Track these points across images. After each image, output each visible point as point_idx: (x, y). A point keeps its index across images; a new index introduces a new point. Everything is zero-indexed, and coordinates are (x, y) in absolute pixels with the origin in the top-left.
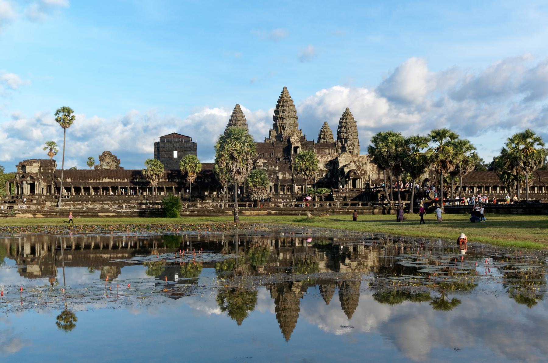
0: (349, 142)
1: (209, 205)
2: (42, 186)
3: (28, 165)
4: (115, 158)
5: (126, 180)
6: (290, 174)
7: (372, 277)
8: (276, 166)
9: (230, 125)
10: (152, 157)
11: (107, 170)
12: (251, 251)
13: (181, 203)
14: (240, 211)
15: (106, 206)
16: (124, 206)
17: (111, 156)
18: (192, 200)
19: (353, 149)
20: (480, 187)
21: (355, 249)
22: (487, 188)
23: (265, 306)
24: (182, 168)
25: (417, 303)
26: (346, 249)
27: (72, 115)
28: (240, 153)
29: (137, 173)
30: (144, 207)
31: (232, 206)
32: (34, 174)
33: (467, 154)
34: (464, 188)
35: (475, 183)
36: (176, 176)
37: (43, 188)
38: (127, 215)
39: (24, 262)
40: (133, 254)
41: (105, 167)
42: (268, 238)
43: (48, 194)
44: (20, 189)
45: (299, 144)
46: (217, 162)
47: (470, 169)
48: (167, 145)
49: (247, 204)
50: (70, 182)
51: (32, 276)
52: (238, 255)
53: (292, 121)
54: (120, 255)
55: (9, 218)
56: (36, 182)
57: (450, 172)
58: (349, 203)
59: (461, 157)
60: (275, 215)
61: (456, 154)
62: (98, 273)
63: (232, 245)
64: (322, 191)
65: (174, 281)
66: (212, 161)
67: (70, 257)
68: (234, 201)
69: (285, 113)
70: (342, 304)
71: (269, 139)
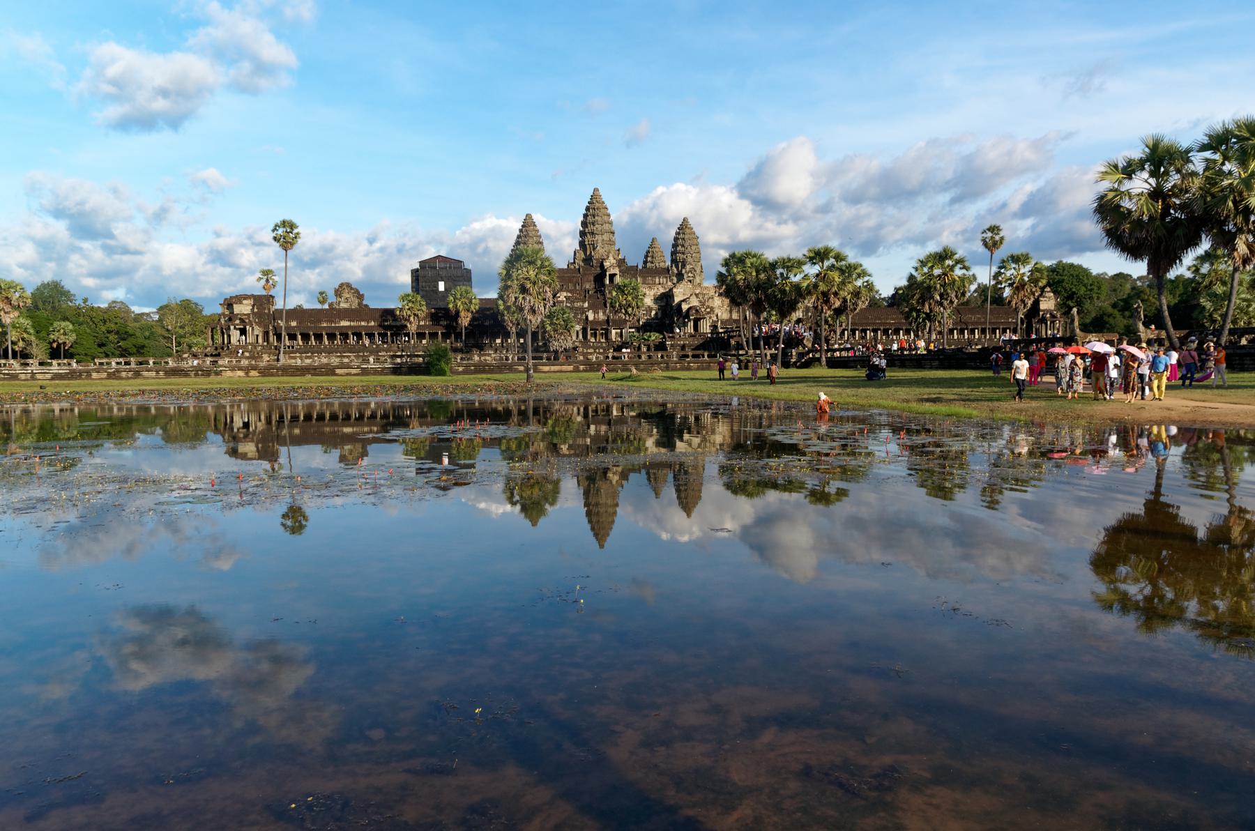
0: (688, 267)
1: (490, 357)
4: (357, 291)
7: (721, 458)
9: (517, 243)
10: (409, 291)
11: (345, 309)
12: (550, 422)
13: (451, 355)
14: (535, 366)
15: (346, 360)
16: (371, 360)
18: (466, 350)
20: (875, 331)
21: (697, 419)
22: (885, 332)
23: (570, 499)
24: (451, 306)
25: (787, 494)
26: (685, 419)
27: (295, 231)
28: (534, 283)
29: (388, 313)
30: (399, 360)
31: (524, 358)
33: (859, 283)
34: (853, 331)
35: (869, 324)
36: (443, 317)
38: (376, 372)
39: (235, 438)
40: (385, 429)
42: (574, 404)
46: (501, 297)
47: (862, 305)
48: (430, 273)
49: (545, 355)
52: (533, 428)
54: (366, 429)
57: (835, 310)
59: (850, 287)
61: (843, 283)
62: (336, 453)
63: (523, 414)
65: (443, 462)
66: (493, 295)
67: (297, 431)
68: (525, 351)
70: (679, 497)
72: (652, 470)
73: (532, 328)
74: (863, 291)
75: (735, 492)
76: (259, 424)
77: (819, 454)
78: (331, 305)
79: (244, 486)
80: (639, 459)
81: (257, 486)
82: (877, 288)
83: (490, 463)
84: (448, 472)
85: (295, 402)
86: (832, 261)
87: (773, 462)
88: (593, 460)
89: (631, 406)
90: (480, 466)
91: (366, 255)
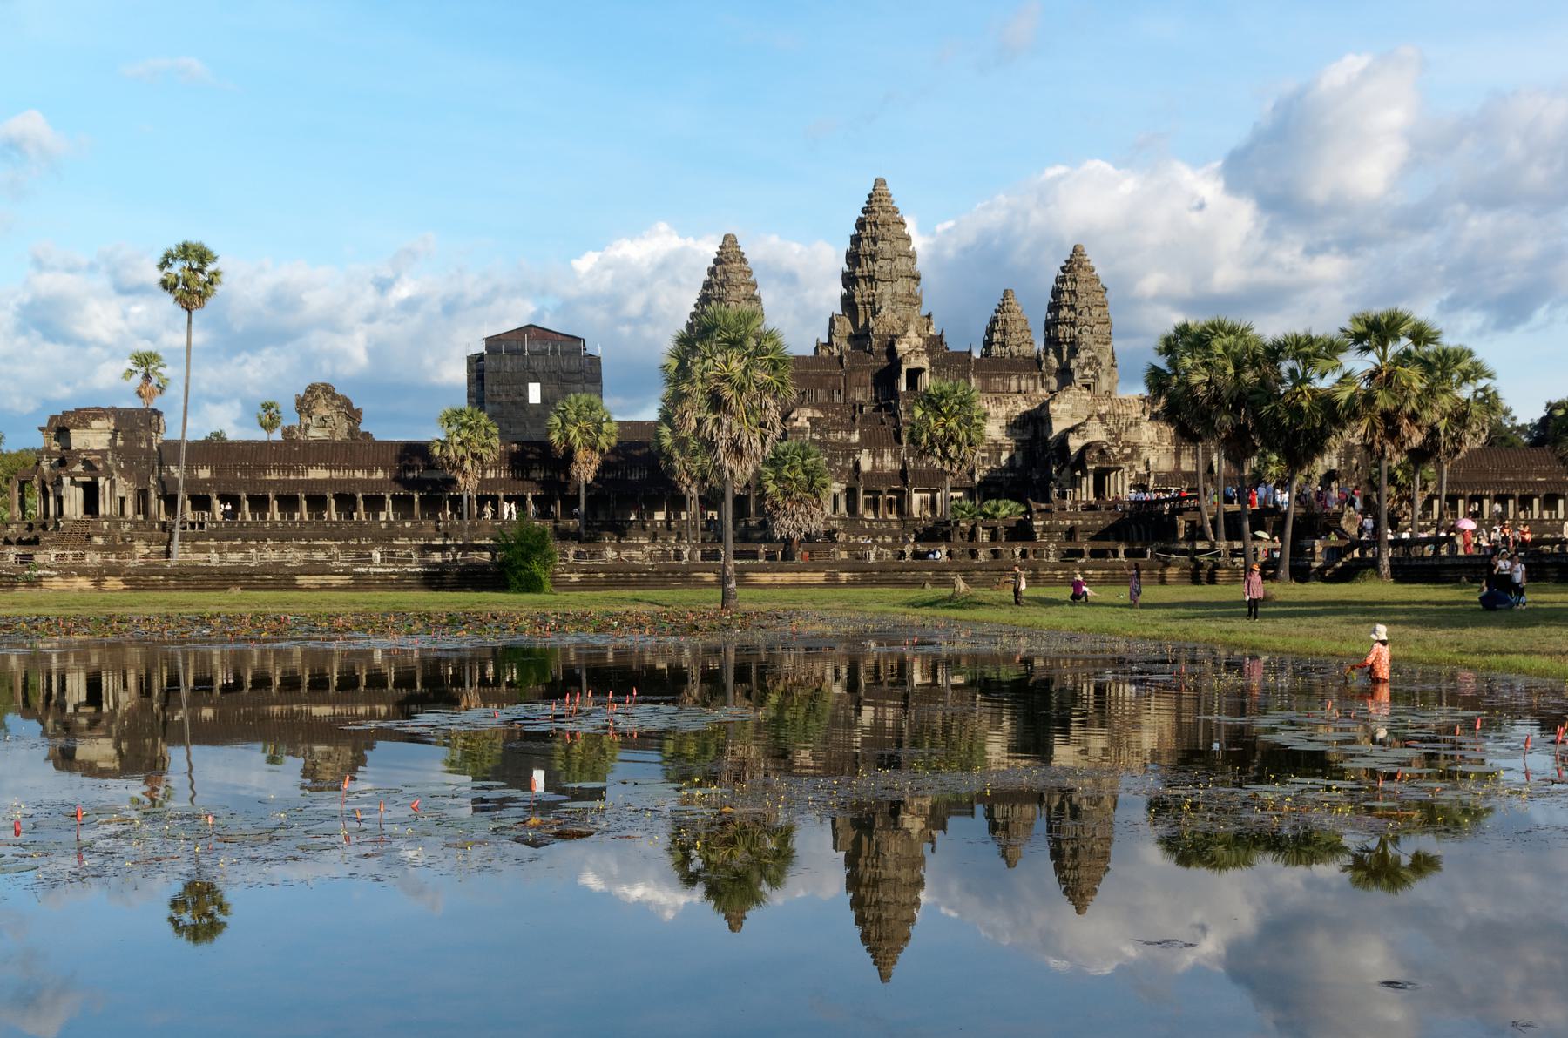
0: (1083, 355)
1: (641, 552)
2: (120, 492)
3: (77, 427)
4: (347, 403)
5: (380, 475)
6: (896, 455)
8: (851, 430)
9: (704, 299)
10: (462, 402)
11: (320, 443)
12: (774, 699)
13: (554, 545)
15: (320, 556)
16: (376, 555)
17: (334, 396)
18: (588, 536)
19: (1096, 377)
20: (1502, 499)
21: (1100, 690)
23: (817, 879)
24: (555, 437)
27: (210, 268)
29: (415, 452)
30: (437, 557)
31: (715, 555)
32: (96, 452)
33: (1466, 392)
34: (1452, 500)
35: (1486, 485)
36: (538, 462)
37: (123, 500)
38: (385, 583)
39: (68, 728)
40: (405, 709)
41: (316, 433)
42: (826, 658)
43: (140, 517)
44: (51, 500)
45: (923, 362)
46: (666, 418)
47: (1472, 442)
48: (509, 364)
49: (763, 548)
50: (205, 481)
51: (90, 769)
52: (734, 710)
53: (901, 287)
54: (362, 710)
55: (21, 592)
56: (101, 480)
58: (1086, 548)
59: (1445, 402)
60: (849, 584)
61: (1430, 392)
62: (293, 765)
63: (712, 680)
64: (997, 509)
65: (534, 788)
66: (651, 414)
67: (208, 713)
68: (720, 540)
69: (881, 262)
70: (1059, 868)
71: (830, 343)
72: (999, 810)
73: (735, 488)
74: (1476, 411)
75: (1184, 860)
76: (124, 697)
77: (1373, 773)
78: (288, 432)
79: (86, 835)
80: (970, 783)
81: (116, 835)
82: (1506, 402)
83: (640, 791)
84: (542, 807)
85: (204, 648)
86: (1405, 342)
87: (1268, 792)
88: (870, 784)
89: (953, 663)
90: (615, 795)
91: (371, 319)
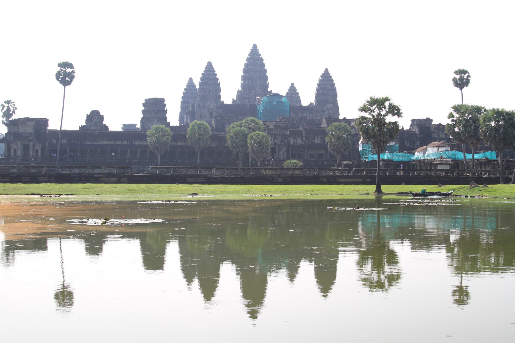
5: (125, 143)
6: (302, 139)
8: (286, 129)
37: (37, 151)
